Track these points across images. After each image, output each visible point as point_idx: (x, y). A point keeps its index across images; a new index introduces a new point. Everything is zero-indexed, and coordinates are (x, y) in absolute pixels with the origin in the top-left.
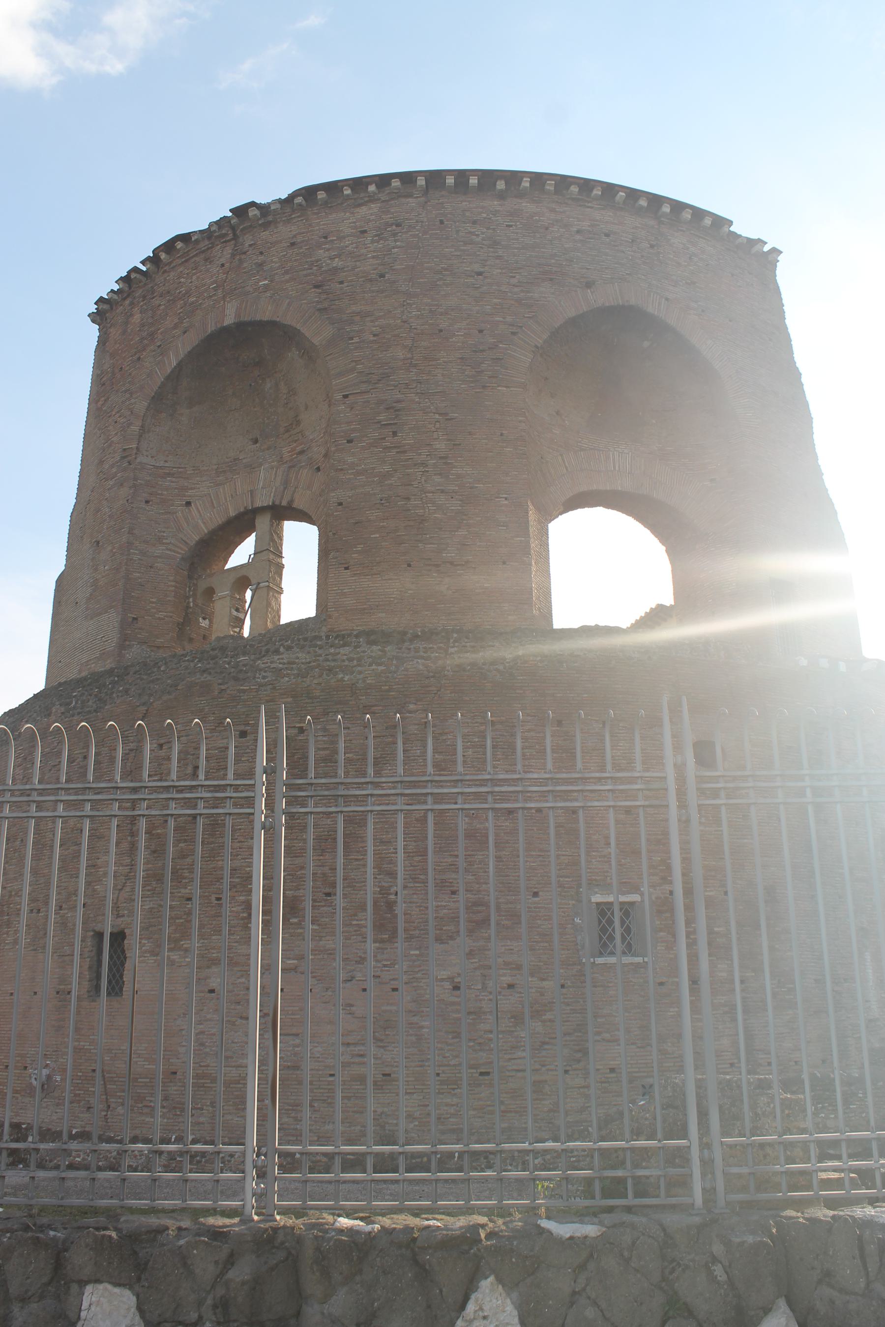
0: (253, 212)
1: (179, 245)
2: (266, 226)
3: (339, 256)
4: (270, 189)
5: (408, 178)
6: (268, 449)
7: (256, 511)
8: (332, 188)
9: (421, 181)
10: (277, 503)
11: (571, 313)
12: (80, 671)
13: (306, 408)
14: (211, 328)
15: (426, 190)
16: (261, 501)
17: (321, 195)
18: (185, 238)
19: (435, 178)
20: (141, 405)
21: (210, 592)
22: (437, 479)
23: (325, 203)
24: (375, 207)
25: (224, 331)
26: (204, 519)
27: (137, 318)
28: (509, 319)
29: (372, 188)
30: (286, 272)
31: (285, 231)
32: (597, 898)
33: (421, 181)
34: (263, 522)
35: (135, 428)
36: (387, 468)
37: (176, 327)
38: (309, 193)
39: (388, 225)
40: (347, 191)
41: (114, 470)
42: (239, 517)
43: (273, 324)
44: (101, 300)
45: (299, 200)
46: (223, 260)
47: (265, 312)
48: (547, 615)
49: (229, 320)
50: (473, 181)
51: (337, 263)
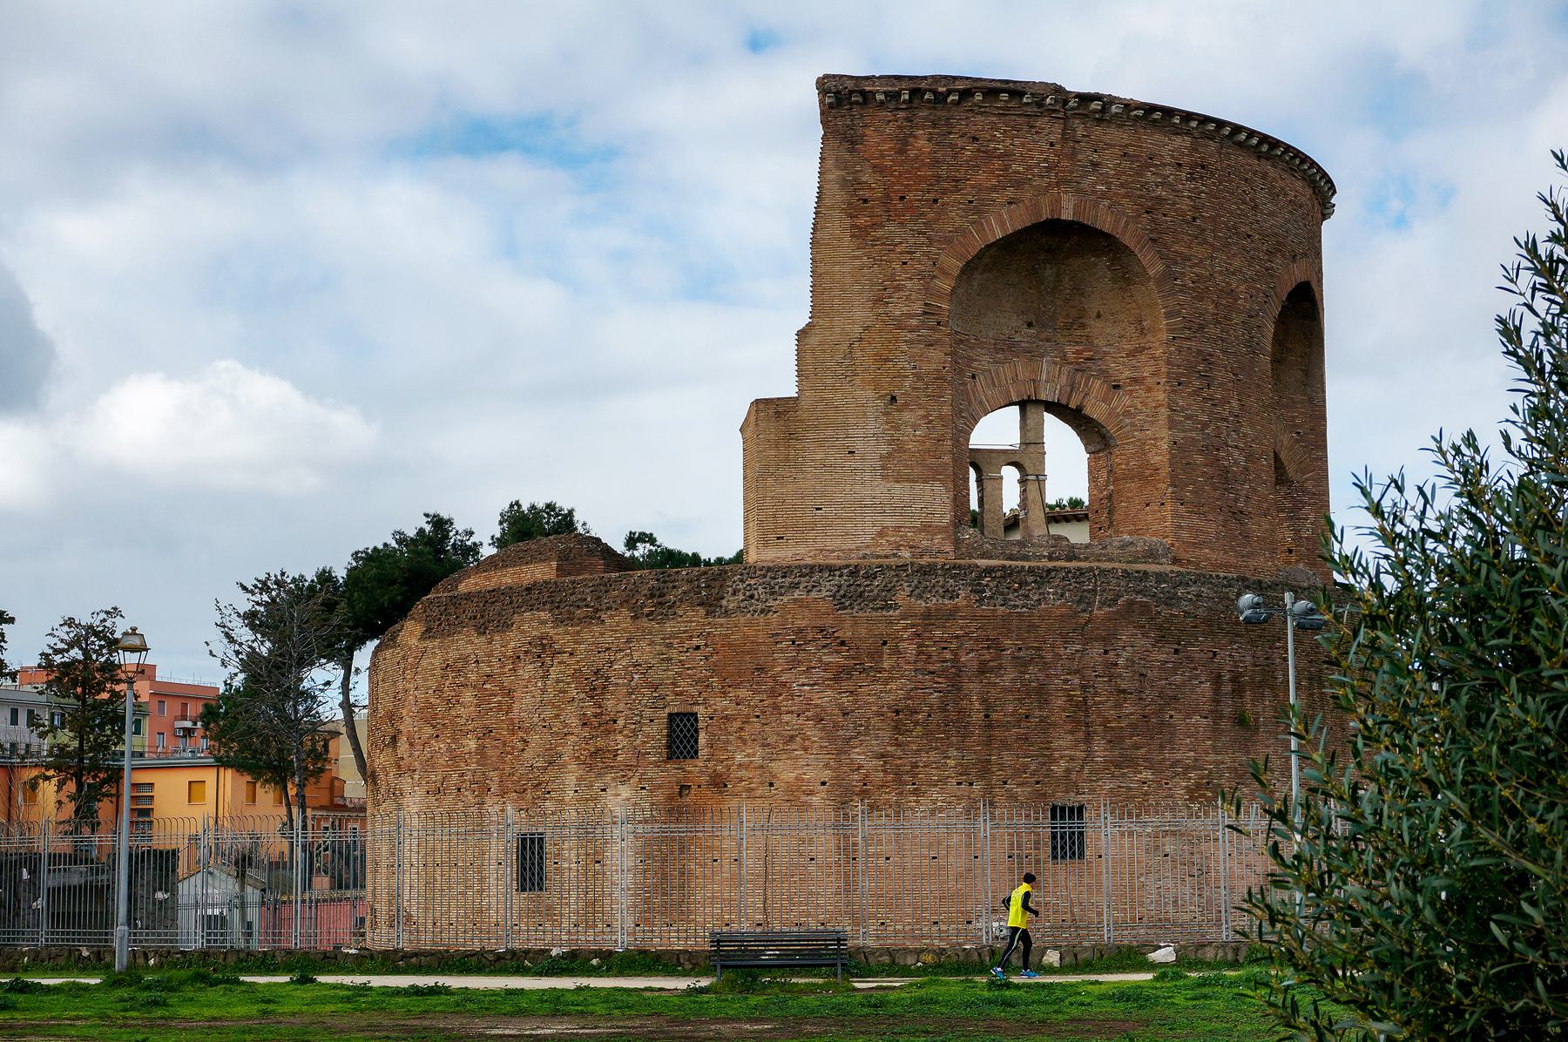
1: (1004, 96)
2: (1100, 121)
3: (1162, 184)
6: (1048, 340)
7: (1038, 402)
8: (1168, 112)
10: (1064, 402)
12: (881, 534)
13: (1099, 316)
14: (1046, 215)
20: (955, 265)
27: (922, 143)
30: (1122, 185)
35: (946, 285)
36: (1205, 418)
37: (994, 189)
41: (914, 322)
46: (1052, 138)
47: (1105, 222)
51: (1159, 191)
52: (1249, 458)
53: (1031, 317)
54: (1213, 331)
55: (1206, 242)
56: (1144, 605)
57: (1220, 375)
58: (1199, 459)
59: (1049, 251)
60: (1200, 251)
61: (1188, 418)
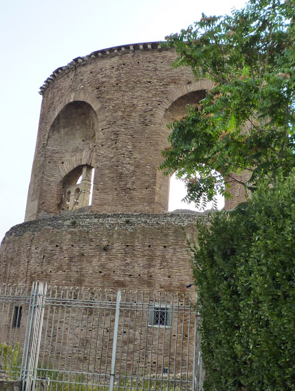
0: (80, 61)
1: (60, 71)
2: (84, 65)
4: (84, 52)
5: (127, 47)
7: (82, 167)
8: (103, 52)
9: (132, 48)
11: (181, 95)
15: (134, 51)
16: (84, 163)
17: (100, 54)
18: (61, 69)
19: (136, 46)
20: (48, 128)
21: (69, 192)
22: (128, 159)
23: (102, 57)
24: (117, 58)
25: (70, 104)
26: (67, 168)
28: (158, 99)
29: (116, 51)
31: (89, 67)
32: (157, 306)
33: (132, 48)
34: (84, 170)
35: (46, 136)
38: (96, 53)
39: (121, 64)
40: (108, 53)
42: (77, 167)
43: (83, 103)
44: (41, 88)
45: (93, 56)
47: (82, 98)
48: (165, 206)
49: (71, 101)
50: (149, 46)
51: (104, 80)
52: (137, 166)
53: (84, 138)
54: (120, 122)
55: (122, 91)
56: (49, 230)
57: (121, 138)
58: (107, 171)
59: (84, 114)
60: (118, 95)
61: (104, 157)
